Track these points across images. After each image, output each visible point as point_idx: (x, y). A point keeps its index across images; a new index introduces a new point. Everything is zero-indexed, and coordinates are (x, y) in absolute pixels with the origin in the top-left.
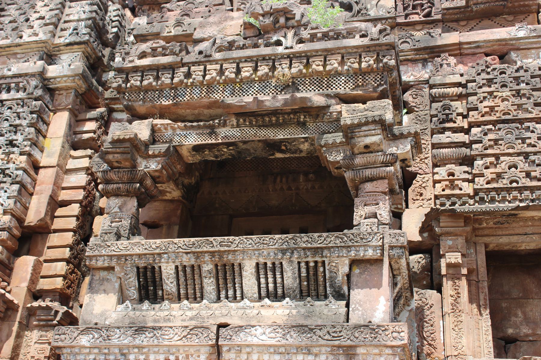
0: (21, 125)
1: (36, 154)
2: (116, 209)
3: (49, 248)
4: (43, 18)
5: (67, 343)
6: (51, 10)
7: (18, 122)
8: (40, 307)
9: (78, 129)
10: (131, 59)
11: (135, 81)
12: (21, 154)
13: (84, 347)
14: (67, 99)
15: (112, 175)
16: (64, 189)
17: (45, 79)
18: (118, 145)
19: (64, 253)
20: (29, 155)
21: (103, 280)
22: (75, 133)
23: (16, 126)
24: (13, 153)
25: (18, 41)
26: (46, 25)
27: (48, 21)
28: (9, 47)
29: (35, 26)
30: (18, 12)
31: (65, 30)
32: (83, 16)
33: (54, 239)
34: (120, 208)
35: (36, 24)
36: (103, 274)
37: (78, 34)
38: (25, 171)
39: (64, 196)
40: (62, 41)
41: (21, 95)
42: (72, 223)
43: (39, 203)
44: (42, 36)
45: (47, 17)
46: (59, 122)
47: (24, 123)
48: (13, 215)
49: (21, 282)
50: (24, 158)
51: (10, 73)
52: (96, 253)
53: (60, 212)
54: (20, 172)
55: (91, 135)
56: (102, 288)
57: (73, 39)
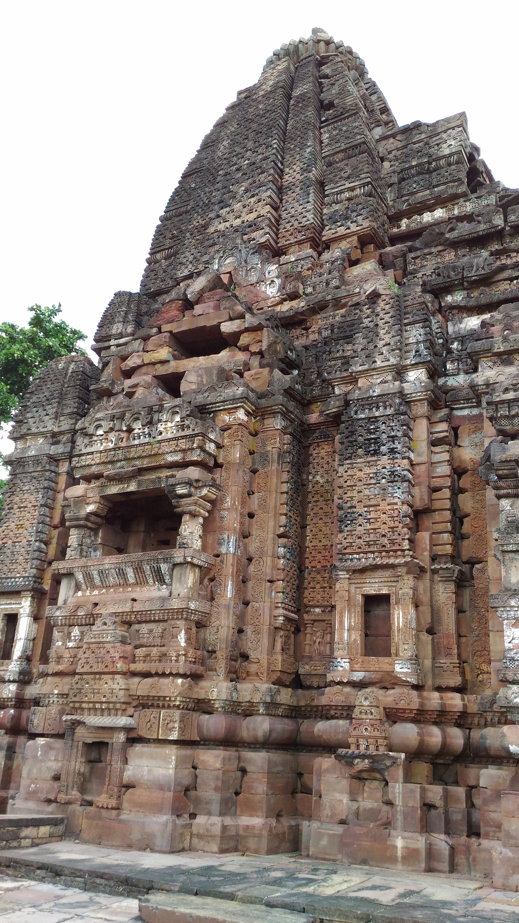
0: (397, 436)
1: (412, 455)
2: (508, 508)
3: (433, 523)
4: (389, 344)
5: (502, 604)
6: (393, 337)
7: (393, 434)
8: (441, 568)
9: (433, 430)
10: (497, 394)
11: (502, 412)
12: (403, 458)
13: (514, 607)
14: (422, 409)
15: (501, 484)
16: (433, 477)
17: (403, 395)
18: (503, 464)
19: (447, 527)
20: (409, 458)
21: (512, 560)
22: (432, 433)
23: (393, 437)
24: (397, 458)
25: (373, 366)
26: (393, 350)
27: (394, 347)
28: (367, 370)
29: (384, 352)
30: (365, 341)
31: (408, 352)
32: (421, 339)
33: (437, 517)
34: (511, 506)
35: (384, 350)
36: (511, 555)
37: (420, 355)
38: (408, 470)
39: (436, 483)
40: (408, 362)
41: (390, 411)
42: (447, 504)
43: (421, 492)
44: (393, 361)
45: (392, 343)
46: (421, 429)
47: (399, 434)
48: (408, 505)
49: (423, 551)
50: (406, 461)
51: (375, 394)
52: (506, 542)
53: (436, 495)
54: (406, 473)
55: (445, 434)
56: (513, 565)
57: (418, 360)
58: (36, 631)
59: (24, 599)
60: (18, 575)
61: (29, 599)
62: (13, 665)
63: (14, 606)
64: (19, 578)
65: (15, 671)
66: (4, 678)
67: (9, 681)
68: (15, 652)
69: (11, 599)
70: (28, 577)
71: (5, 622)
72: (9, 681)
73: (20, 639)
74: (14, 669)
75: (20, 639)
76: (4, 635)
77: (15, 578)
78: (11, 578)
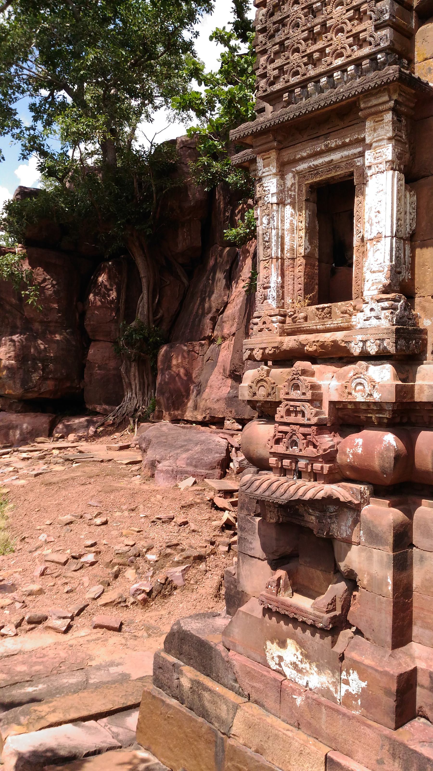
58: (414, 215)
59: (369, 124)
60: (339, 62)
61: (389, 117)
62: (368, 313)
63: (336, 156)
64: (343, 68)
65: (377, 328)
66: (346, 350)
67: (365, 357)
68: (368, 276)
69: (326, 136)
70: (372, 57)
71: (313, 206)
72: (365, 357)
73: (378, 238)
74: (374, 322)
75: (378, 238)
76: (316, 242)
77: (329, 74)
78: (316, 79)
